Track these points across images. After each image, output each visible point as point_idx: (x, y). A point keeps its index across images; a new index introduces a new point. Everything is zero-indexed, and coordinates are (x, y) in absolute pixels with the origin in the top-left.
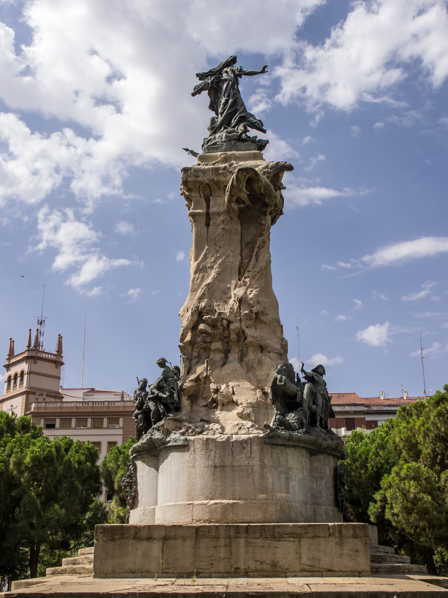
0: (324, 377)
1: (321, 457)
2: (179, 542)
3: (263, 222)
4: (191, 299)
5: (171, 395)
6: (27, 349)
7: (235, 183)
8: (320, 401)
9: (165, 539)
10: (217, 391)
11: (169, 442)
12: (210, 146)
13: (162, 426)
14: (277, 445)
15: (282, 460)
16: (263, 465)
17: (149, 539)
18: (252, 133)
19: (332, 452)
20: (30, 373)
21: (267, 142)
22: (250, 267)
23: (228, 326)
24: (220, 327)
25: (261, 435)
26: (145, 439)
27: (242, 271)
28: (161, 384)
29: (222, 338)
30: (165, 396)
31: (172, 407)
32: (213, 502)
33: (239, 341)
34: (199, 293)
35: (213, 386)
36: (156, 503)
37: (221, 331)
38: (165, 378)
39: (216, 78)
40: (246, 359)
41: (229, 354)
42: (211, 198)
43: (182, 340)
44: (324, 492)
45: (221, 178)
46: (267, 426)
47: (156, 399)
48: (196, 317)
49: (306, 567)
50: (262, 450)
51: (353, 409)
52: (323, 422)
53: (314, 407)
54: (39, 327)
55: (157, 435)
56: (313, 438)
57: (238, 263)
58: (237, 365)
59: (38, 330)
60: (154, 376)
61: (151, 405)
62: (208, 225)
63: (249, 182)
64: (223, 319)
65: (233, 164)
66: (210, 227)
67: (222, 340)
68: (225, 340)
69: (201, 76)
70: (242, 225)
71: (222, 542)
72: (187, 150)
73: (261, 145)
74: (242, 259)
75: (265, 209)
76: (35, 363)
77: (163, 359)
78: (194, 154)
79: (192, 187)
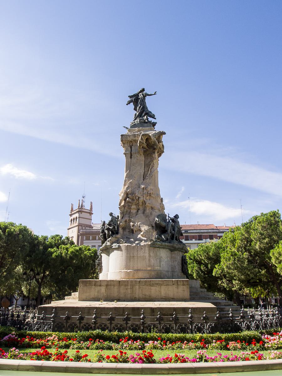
0: (179, 219)
1: (176, 252)
2: (112, 287)
3: (153, 156)
4: (124, 188)
5: (114, 228)
6: (78, 208)
7: (141, 140)
8: (176, 229)
9: (107, 285)
10: (133, 226)
11: (113, 246)
12: (134, 126)
13: (110, 240)
14: (156, 247)
15: (158, 254)
16: (150, 256)
17: (100, 286)
18: (150, 119)
19: (181, 250)
20: (79, 217)
21: (156, 123)
22: (148, 175)
23: (138, 199)
25: (150, 244)
26: (104, 245)
27: (145, 176)
28: (110, 223)
29: (136, 204)
30: (111, 228)
31: (114, 232)
32: (129, 271)
33: (143, 205)
34: (126, 187)
35: (131, 224)
36: (108, 271)
37: (136, 201)
38: (112, 221)
39: (136, 97)
40: (146, 212)
41: (139, 211)
42: (132, 147)
43: (120, 205)
44: (177, 267)
45: (136, 138)
46: (151, 240)
47: (108, 229)
48: (125, 196)
49: (163, 297)
50: (149, 250)
51: (212, 231)
52: (177, 238)
53: (173, 232)
54: (83, 199)
55: (108, 244)
56: (171, 244)
57: (143, 173)
58: (142, 215)
59: (82, 200)
60: (108, 219)
61: (106, 231)
62: (131, 158)
63: (147, 140)
64: (136, 196)
65: (141, 132)
66: (132, 159)
67: (136, 205)
68: (137, 205)
69: (130, 97)
70: (145, 157)
71: (129, 287)
72: (125, 127)
73: (154, 124)
74: (145, 171)
75: (154, 151)
76: (81, 214)
77: (111, 213)
78: (127, 128)
79: (125, 143)
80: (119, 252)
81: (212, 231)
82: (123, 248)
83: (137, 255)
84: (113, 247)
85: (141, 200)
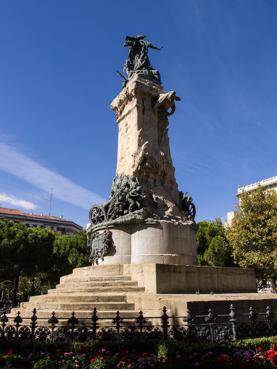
2: (193, 274)
9: (187, 272)
11: (147, 221)
17: (180, 272)
24: (154, 167)
32: (173, 255)
36: (130, 253)
42: (144, 100)
49: (238, 288)
51: (19, 217)
58: (161, 187)
64: (156, 163)
66: (144, 115)
68: (156, 174)
70: (158, 119)
71: (209, 275)
80: (158, 230)
81: (19, 217)
82: (164, 226)
83: (181, 236)
84: (147, 223)
85: (161, 169)
